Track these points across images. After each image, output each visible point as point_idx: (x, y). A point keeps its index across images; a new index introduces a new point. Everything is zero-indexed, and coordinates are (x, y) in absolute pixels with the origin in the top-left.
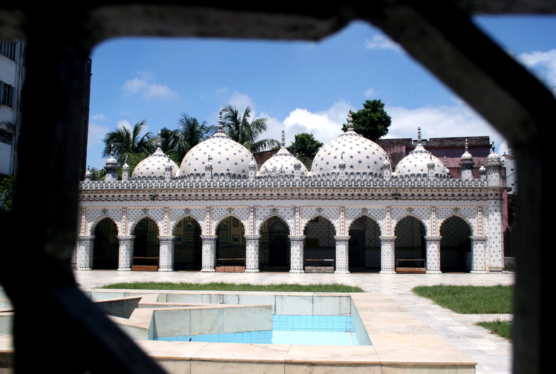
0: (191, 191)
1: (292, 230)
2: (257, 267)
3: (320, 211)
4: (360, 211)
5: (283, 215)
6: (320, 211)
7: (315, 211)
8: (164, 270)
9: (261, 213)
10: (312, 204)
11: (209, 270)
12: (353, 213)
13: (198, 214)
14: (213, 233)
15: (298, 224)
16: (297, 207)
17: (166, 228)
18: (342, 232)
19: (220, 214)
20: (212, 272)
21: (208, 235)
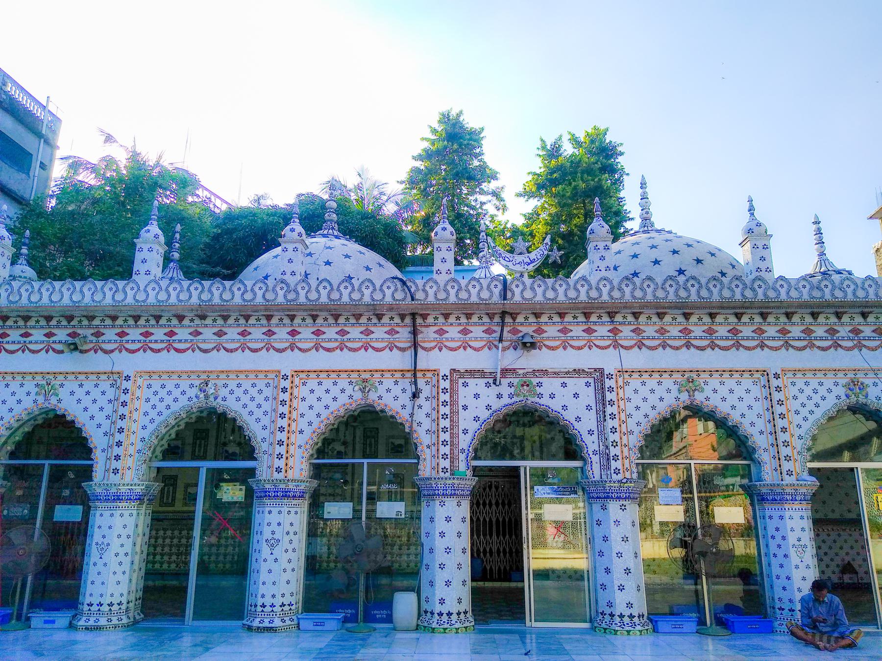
0: (225, 318)
1: (595, 459)
2: (466, 605)
3: (691, 392)
4: (841, 391)
5: (555, 405)
6: (691, 392)
7: (674, 388)
8: (91, 623)
9: (477, 396)
10: (663, 366)
11: (277, 623)
12: (816, 398)
13: (245, 399)
14: (298, 468)
15: (616, 437)
16: (610, 377)
17: (116, 451)
18: (786, 466)
19: (327, 399)
20: (286, 629)
21: (281, 476)
